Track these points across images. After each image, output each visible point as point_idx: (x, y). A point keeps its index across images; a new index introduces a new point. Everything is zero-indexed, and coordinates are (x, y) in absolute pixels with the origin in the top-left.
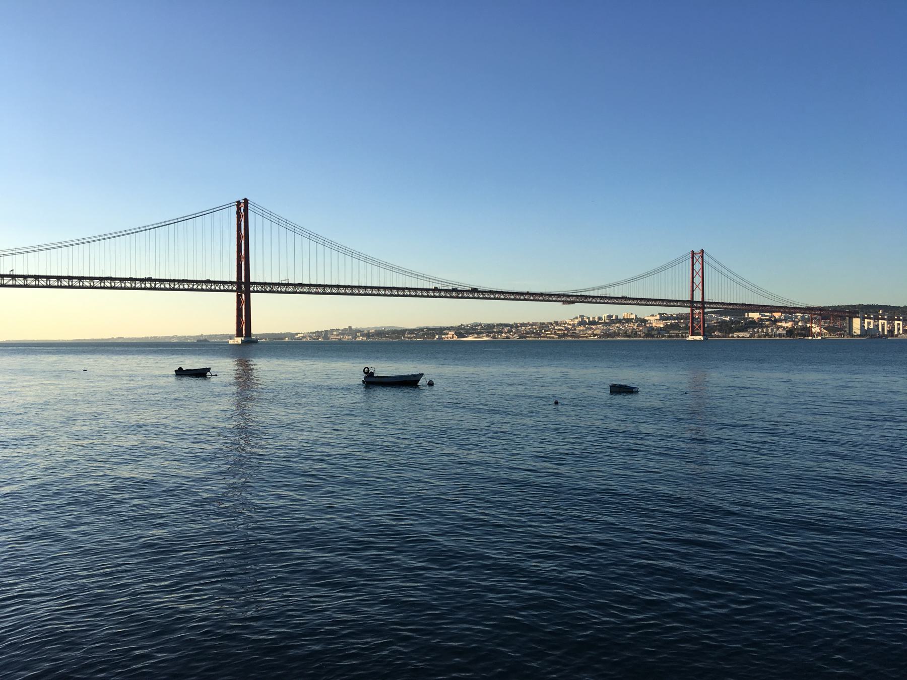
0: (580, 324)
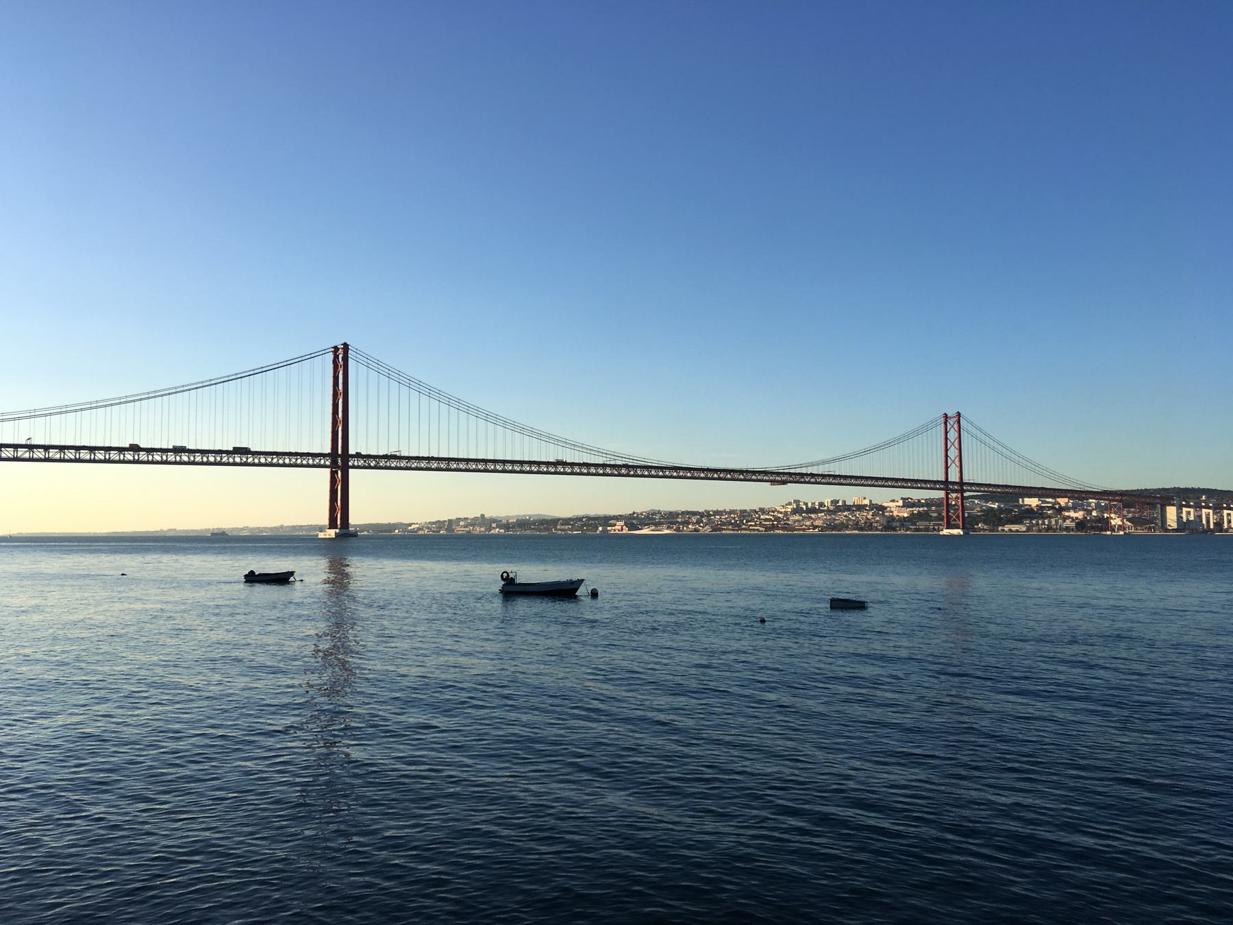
0: (794, 512)
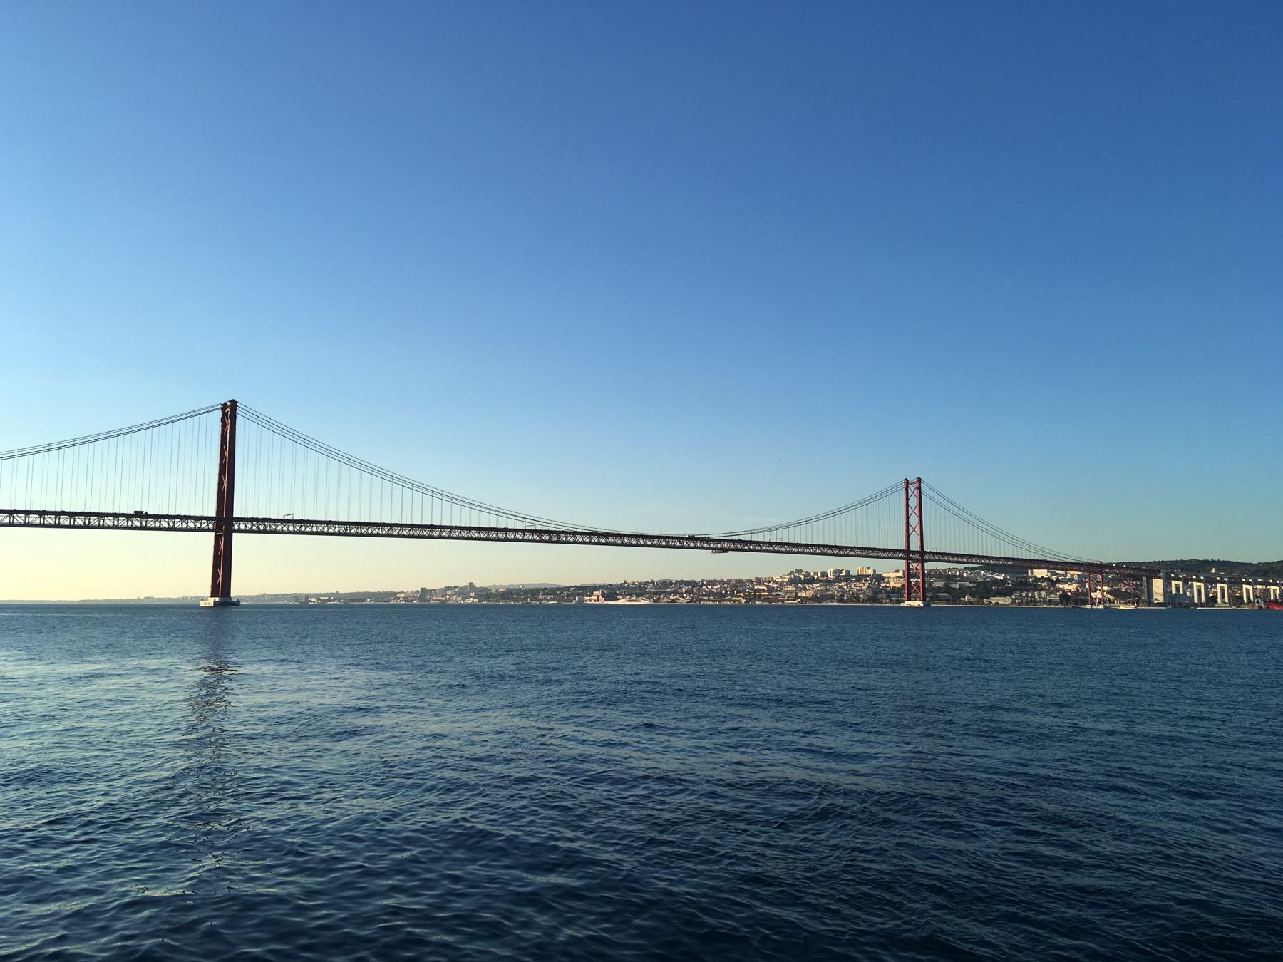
0: (791, 582)
